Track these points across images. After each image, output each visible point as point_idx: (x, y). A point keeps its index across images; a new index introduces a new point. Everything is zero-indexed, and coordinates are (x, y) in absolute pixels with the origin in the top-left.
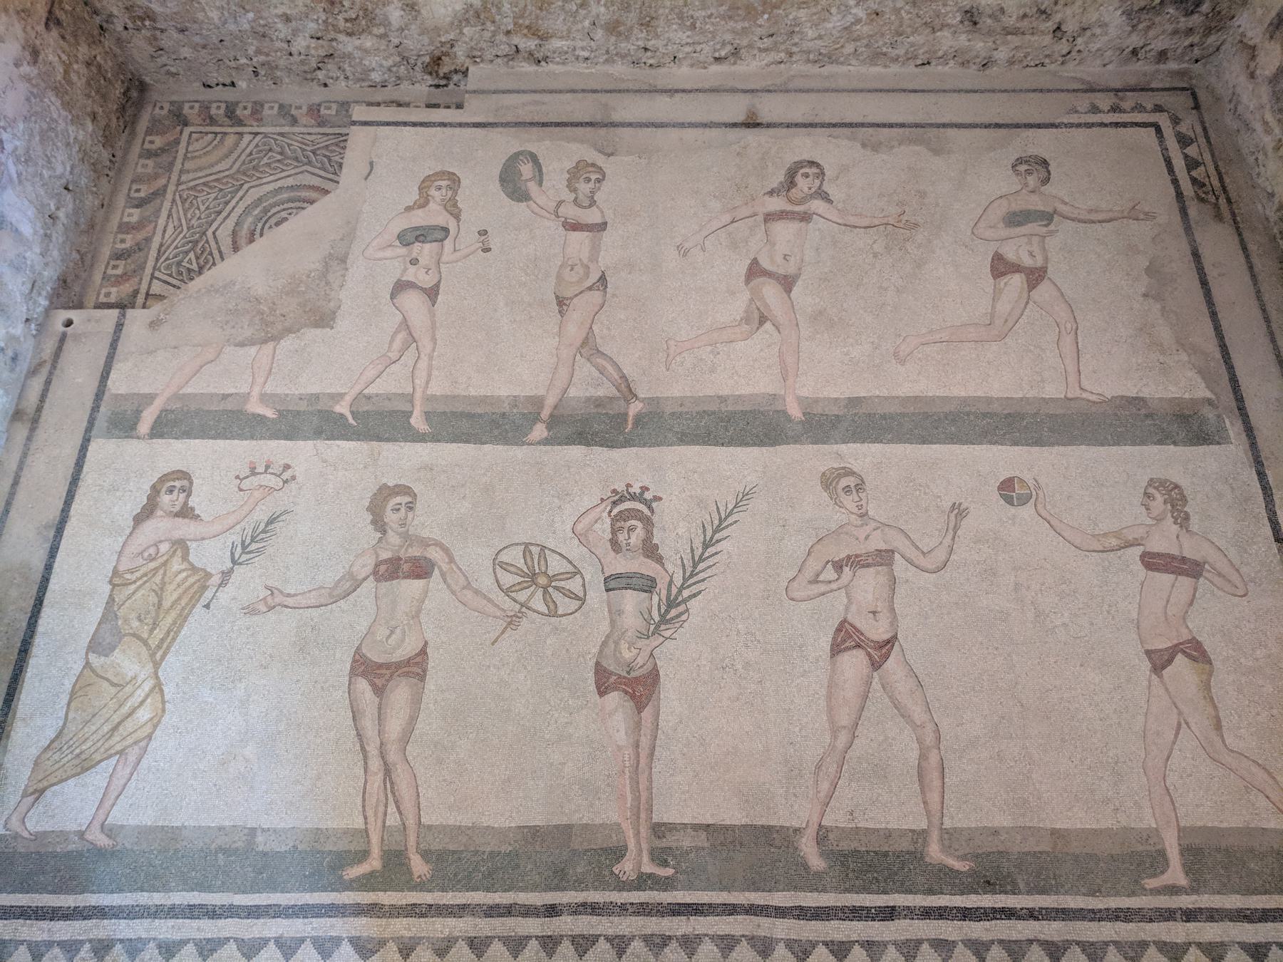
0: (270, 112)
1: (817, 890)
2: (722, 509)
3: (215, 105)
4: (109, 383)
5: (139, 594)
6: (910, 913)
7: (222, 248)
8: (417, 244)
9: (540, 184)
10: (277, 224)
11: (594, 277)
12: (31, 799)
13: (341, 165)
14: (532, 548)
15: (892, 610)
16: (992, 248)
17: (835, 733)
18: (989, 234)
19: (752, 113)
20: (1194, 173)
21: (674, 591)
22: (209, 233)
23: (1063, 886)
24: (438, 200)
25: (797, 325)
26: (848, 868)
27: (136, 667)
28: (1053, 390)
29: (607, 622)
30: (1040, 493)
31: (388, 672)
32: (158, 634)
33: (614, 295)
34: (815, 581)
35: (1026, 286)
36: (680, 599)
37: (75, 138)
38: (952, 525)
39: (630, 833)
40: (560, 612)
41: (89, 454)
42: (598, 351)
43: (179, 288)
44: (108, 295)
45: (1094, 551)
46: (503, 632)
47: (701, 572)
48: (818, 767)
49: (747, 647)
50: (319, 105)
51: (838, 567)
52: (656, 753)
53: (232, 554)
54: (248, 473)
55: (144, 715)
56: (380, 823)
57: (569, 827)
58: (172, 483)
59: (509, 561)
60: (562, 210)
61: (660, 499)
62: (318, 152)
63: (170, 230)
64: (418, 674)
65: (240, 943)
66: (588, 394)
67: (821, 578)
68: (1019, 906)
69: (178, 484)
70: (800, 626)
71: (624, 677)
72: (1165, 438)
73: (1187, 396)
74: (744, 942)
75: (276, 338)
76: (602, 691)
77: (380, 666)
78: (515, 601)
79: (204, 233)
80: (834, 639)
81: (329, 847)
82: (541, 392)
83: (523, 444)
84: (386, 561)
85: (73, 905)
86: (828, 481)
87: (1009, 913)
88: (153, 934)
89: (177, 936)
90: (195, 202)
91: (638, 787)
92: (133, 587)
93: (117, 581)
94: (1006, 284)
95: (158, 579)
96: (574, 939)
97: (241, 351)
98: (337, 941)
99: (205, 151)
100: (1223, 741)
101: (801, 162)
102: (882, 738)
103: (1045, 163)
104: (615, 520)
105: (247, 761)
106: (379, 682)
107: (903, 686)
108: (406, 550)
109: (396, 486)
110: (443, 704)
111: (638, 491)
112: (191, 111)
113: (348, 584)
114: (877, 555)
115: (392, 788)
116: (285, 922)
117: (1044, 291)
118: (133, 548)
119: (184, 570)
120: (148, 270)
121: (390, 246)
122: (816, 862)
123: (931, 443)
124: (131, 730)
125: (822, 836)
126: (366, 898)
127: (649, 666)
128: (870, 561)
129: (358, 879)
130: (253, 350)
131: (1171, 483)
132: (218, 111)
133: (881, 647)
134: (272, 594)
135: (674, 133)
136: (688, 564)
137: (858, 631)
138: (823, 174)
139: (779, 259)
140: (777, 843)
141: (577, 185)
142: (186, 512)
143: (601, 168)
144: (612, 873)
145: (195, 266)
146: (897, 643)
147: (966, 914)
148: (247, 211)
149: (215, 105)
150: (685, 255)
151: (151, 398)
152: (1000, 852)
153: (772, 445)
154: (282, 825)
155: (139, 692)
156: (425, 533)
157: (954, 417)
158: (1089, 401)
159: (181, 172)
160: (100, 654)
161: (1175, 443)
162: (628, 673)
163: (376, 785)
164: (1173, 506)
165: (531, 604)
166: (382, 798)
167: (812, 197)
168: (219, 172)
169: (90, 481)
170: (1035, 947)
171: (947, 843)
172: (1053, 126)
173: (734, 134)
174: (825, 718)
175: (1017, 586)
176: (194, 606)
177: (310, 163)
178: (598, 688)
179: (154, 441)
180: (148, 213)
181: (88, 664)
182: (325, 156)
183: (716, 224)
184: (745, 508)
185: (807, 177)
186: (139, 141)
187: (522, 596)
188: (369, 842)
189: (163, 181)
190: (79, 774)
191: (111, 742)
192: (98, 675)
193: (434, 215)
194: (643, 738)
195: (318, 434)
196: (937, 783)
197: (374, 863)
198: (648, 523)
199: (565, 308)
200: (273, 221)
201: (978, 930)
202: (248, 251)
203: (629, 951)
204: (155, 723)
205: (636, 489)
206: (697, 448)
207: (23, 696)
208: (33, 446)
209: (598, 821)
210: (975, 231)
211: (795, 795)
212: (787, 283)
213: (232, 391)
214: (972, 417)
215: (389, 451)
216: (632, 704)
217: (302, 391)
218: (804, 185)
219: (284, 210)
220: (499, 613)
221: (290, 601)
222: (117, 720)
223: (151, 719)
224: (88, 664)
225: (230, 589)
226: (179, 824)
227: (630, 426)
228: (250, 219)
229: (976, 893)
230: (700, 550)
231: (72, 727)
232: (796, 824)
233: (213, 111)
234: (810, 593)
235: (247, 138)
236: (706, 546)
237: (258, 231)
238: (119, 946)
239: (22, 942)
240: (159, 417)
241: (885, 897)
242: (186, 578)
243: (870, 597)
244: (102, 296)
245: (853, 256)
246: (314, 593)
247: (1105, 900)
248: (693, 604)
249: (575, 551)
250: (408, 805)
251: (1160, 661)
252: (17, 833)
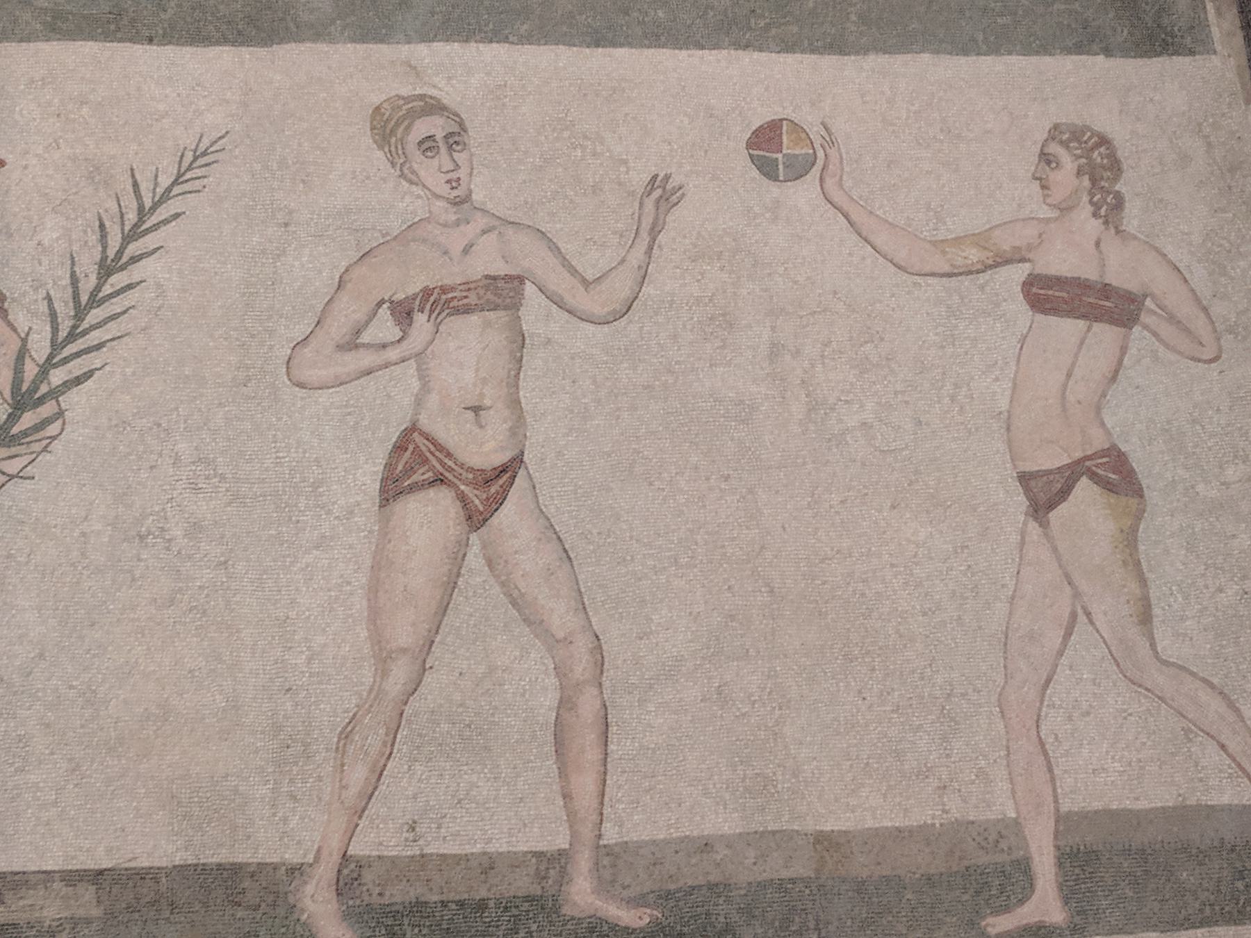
15: (515, 403)
30: (833, 152)
34: (351, 344)
70: (315, 442)
80: (389, 466)
102: (481, 669)
133: (488, 482)
136: (65, 311)
140: (251, 897)
146: (522, 473)
230: (93, 280)
243: (469, 376)
248: (74, 400)
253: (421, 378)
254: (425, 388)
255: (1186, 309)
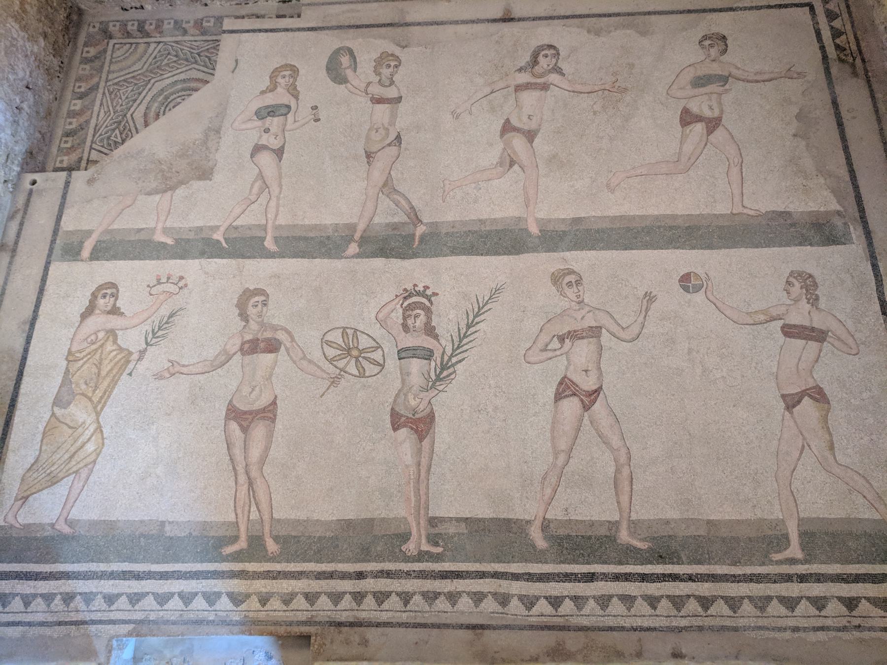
0: (168, 26)
1: (541, 562)
2: (480, 300)
3: (130, 23)
4: (62, 223)
5: (85, 367)
6: (605, 577)
7: (138, 126)
8: (269, 118)
9: (355, 71)
10: (174, 107)
11: (392, 136)
12: (20, 502)
13: (216, 61)
14: (348, 331)
15: (599, 369)
16: (682, 104)
17: (556, 454)
18: (679, 94)
19: (508, 11)
20: (838, 41)
21: (446, 358)
22: (129, 116)
23: (713, 559)
24: (283, 85)
25: (537, 166)
26: (563, 547)
27: (85, 416)
28: (722, 208)
29: (400, 380)
30: (710, 283)
31: (250, 417)
32: (99, 393)
33: (406, 149)
34: (545, 350)
35: (705, 132)
36: (450, 364)
37: (32, 51)
38: (644, 308)
39: (414, 525)
40: (366, 375)
41: (50, 273)
42: (395, 190)
43: (106, 154)
44: (61, 162)
45: (747, 324)
46: (328, 389)
47: (464, 345)
48: (544, 478)
49: (496, 396)
50: (202, 20)
51: (562, 339)
52: (432, 469)
53: (146, 338)
54: (155, 283)
55: (90, 447)
56: (246, 518)
57: (373, 520)
58: (105, 291)
59: (333, 340)
60: (370, 89)
61: (437, 294)
62: (201, 54)
63: (102, 114)
64: (271, 418)
65: (156, 596)
66: (387, 221)
67: (549, 347)
68: (681, 573)
69: (109, 291)
71: (411, 418)
72: (804, 241)
73: (822, 209)
74: (490, 597)
75: (173, 188)
76: (396, 427)
77: (245, 413)
78: (336, 367)
79: (125, 115)
80: (557, 389)
81: (212, 533)
82: (354, 220)
83: (342, 258)
84: (249, 341)
85: (49, 571)
86: (556, 279)
87: (674, 577)
88: (100, 590)
89: (116, 591)
90: (118, 93)
91: (419, 493)
92: (81, 362)
93: (71, 358)
94: (690, 131)
95: (97, 356)
96: (375, 594)
97: (151, 198)
98: (218, 595)
99: (124, 57)
100: (835, 458)
101: (542, 46)
102: (589, 458)
103: (724, 38)
104: (405, 310)
105: (158, 477)
106: (245, 424)
107: (605, 422)
108: (262, 334)
109: (255, 289)
110: (287, 438)
111: (422, 289)
112: (113, 28)
113: (223, 358)
114: (589, 331)
115: (254, 495)
116: (185, 582)
117: (719, 134)
118: (81, 335)
119: (114, 350)
120: (88, 143)
121: (250, 120)
122: (541, 543)
123: (632, 249)
124: (82, 457)
125: (546, 525)
126: (237, 567)
127: (428, 410)
128: (584, 334)
129: (231, 555)
130: (157, 198)
131: (807, 274)
132: (132, 28)
133: (590, 395)
134: (173, 365)
135: (451, 29)
136: (456, 340)
137: (574, 383)
138: (558, 54)
139: (525, 119)
140: (514, 530)
141: (381, 70)
142: (115, 311)
143: (398, 57)
144: (401, 550)
145: (119, 140)
146: (602, 392)
147: (644, 578)
148: (154, 99)
149: (130, 23)
150: (457, 118)
151: (89, 233)
152: (670, 536)
153: (518, 253)
154: (182, 519)
155: (87, 432)
156: (275, 322)
157: (648, 230)
158: (748, 215)
159: (109, 72)
160: (61, 407)
161: (811, 245)
162: (414, 415)
163: (243, 493)
164: (807, 290)
165: (347, 369)
166: (247, 501)
167: (550, 72)
168: (135, 71)
169: (51, 291)
170: (692, 599)
171: (632, 530)
172: (731, 9)
173: (494, 27)
174: (550, 445)
175: (690, 351)
176: (121, 374)
177: (196, 62)
178: (393, 424)
179: (93, 262)
180: (87, 103)
181: (53, 414)
182: (207, 57)
183: (480, 95)
184: (496, 299)
185: (546, 57)
186: (79, 51)
187: (341, 364)
188: (239, 530)
189: (96, 80)
190: (50, 486)
191: (70, 465)
192: (60, 422)
193: (281, 97)
194: (423, 459)
195: (202, 254)
196: (627, 489)
197: (242, 544)
198: (428, 311)
199: (371, 159)
200: (171, 105)
201: (652, 589)
202: (154, 126)
203: (411, 602)
204: (98, 452)
205: (420, 288)
206: (464, 258)
207: (12, 436)
208: (13, 268)
209: (392, 516)
210: (669, 92)
211: (527, 498)
212: (530, 136)
213: (144, 226)
214: (662, 230)
215: (251, 265)
216: (416, 436)
217: (191, 225)
218: (544, 63)
219: (179, 97)
220: (325, 376)
221: (185, 370)
222: (74, 451)
223: (95, 450)
224: (53, 414)
225: (145, 363)
226: (115, 519)
227: (417, 243)
228: (156, 105)
229: (651, 563)
230: (465, 330)
231: (44, 456)
232: (527, 517)
233: (129, 28)
234: (540, 358)
235: (153, 46)
236: (469, 326)
237: (162, 112)
238: (79, 597)
239: (17, 595)
240: (95, 246)
241: (588, 566)
242: (117, 354)
243: (584, 360)
244: (58, 162)
245: (579, 114)
246: (199, 364)
247: (743, 568)
248: (459, 367)
249: (377, 332)
250: (264, 506)
251: (791, 402)
252: (12, 525)
253: (567, 360)
254: (569, 364)
255: (844, 336)
